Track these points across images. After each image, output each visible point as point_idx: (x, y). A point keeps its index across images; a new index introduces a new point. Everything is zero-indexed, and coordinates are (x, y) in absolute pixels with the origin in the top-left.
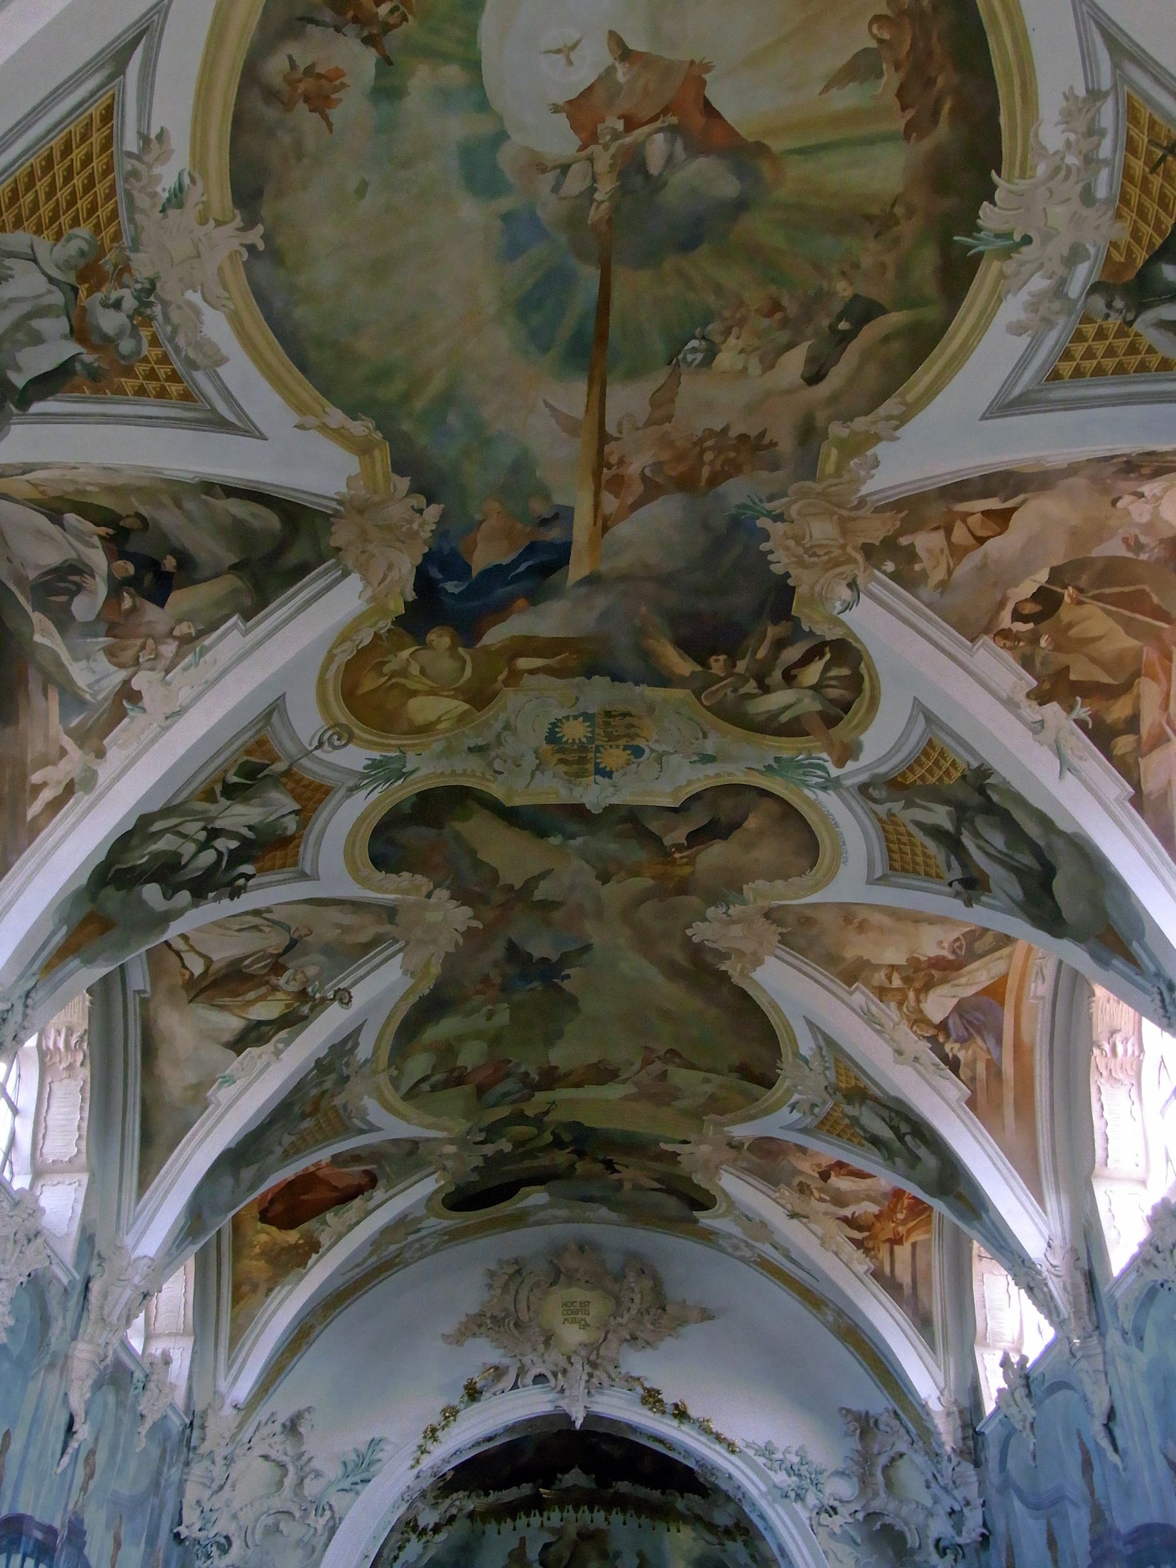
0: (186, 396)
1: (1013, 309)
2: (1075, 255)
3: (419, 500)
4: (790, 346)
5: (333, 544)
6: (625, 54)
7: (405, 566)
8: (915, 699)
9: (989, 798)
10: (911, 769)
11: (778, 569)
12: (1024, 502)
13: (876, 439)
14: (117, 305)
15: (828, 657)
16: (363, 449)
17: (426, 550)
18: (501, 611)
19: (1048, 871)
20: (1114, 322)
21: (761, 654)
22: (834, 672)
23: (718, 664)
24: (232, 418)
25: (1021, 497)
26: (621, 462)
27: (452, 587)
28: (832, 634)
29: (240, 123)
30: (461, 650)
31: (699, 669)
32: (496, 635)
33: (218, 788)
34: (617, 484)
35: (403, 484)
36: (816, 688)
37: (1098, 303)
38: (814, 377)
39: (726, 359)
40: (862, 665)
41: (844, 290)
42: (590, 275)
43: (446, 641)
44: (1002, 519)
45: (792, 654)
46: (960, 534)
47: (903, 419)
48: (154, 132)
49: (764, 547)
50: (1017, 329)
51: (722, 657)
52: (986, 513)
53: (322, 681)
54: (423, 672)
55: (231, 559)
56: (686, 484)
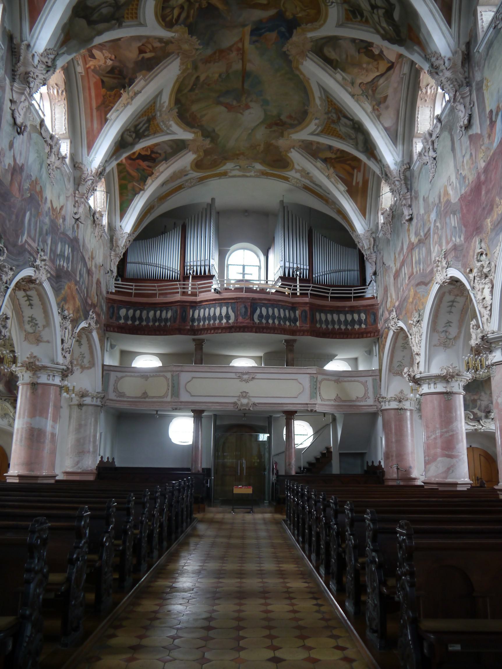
0: (328, 97)
1: (166, 104)
2: (161, 115)
3: (287, 52)
4: (204, 80)
5: (312, 43)
6: (241, 113)
7: (295, 38)
8: (147, 26)
9: (114, 20)
10: (137, 5)
11: (194, 37)
12: (138, 57)
13: (181, 74)
14: (332, 116)
15: (174, 20)
16: (298, 69)
17: (288, 41)
18: (271, 19)
19: (90, 23)
20: (150, 115)
21: (192, 12)
22: (170, 17)
23: (204, 4)
24: (321, 89)
25: (140, 58)
26: (238, 54)
27: (283, 29)
28: (176, 27)
29: (304, 120)
30: (283, 9)
31: (210, 1)
32: (272, 12)
33: (364, 19)
34: (238, 50)
35: (290, 58)
36: (174, 8)
37: (154, 114)
38: (198, 78)
39: (217, 76)
40: (164, 25)
41: (197, 91)
42: (246, 86)
43: (288, 14)
44: (141, 51)
45: (183, 15)
46: (150, 46)
47: (177, 79)
48: (316, 127)
49: (199, 41)
50: (164, 102)
51: (203, 7)
52: (146, 52)
53: (325, 21)
54: (296, 7)
55: (340, 41)
56: (221, 51)
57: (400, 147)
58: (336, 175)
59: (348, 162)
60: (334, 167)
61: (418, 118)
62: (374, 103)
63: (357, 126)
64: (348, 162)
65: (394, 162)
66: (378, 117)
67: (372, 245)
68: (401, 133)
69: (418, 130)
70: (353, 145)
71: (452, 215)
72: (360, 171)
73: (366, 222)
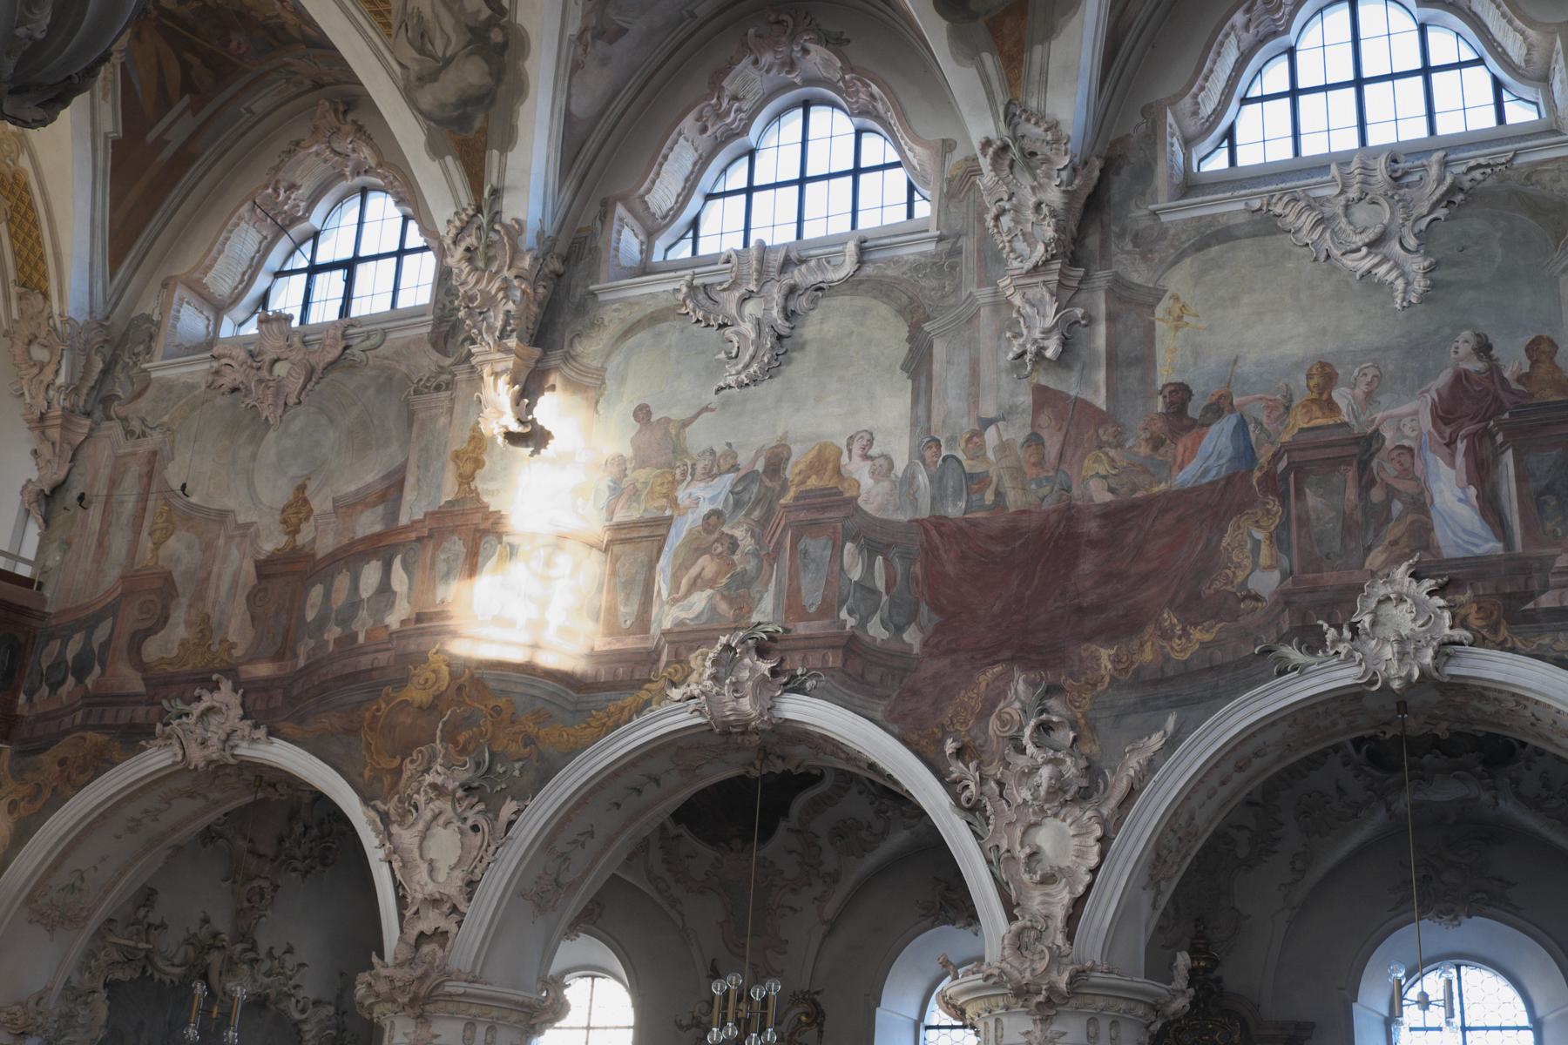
57: (567, 195)
58: (123, 64)
59: (189, 57)
60: (137, 36)
61: (666, 158)
62: (593, 22)
63: (496, 36)
64: (189, 57)
65: (539, 229)
66: (576, 67)
67: (92, 383)
68: (587, 158)
69: (649, 191)
70: (401, 65)
71: (849, 546)
72: (195, 113)
73: (110, 290)
